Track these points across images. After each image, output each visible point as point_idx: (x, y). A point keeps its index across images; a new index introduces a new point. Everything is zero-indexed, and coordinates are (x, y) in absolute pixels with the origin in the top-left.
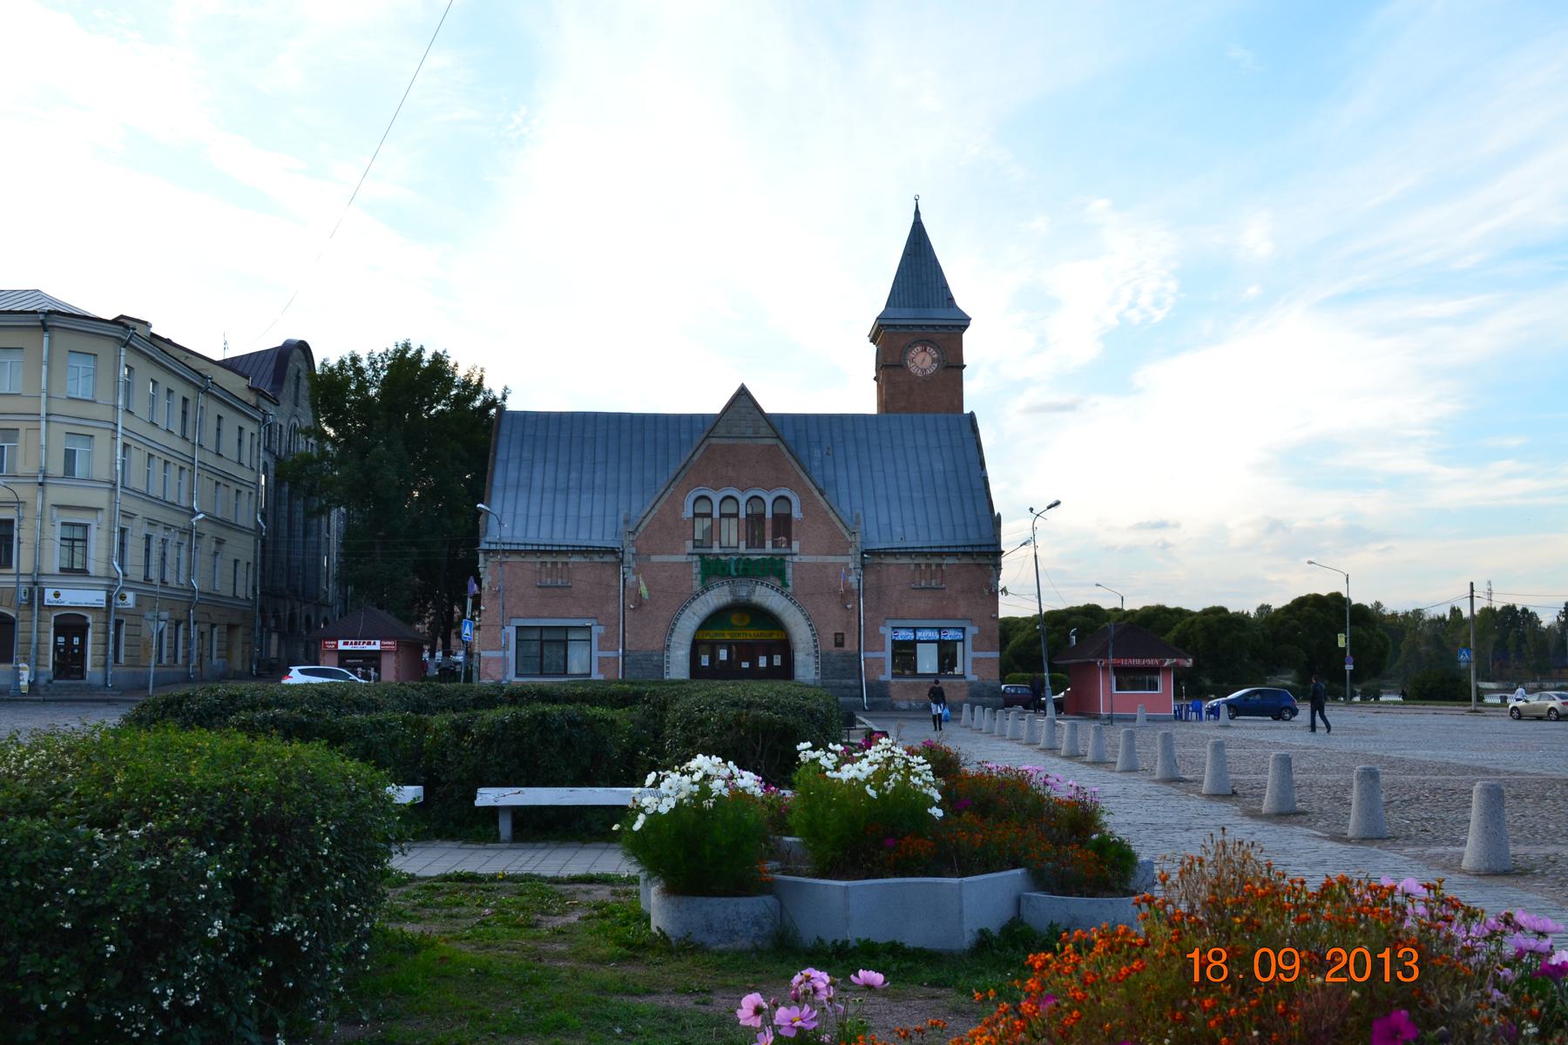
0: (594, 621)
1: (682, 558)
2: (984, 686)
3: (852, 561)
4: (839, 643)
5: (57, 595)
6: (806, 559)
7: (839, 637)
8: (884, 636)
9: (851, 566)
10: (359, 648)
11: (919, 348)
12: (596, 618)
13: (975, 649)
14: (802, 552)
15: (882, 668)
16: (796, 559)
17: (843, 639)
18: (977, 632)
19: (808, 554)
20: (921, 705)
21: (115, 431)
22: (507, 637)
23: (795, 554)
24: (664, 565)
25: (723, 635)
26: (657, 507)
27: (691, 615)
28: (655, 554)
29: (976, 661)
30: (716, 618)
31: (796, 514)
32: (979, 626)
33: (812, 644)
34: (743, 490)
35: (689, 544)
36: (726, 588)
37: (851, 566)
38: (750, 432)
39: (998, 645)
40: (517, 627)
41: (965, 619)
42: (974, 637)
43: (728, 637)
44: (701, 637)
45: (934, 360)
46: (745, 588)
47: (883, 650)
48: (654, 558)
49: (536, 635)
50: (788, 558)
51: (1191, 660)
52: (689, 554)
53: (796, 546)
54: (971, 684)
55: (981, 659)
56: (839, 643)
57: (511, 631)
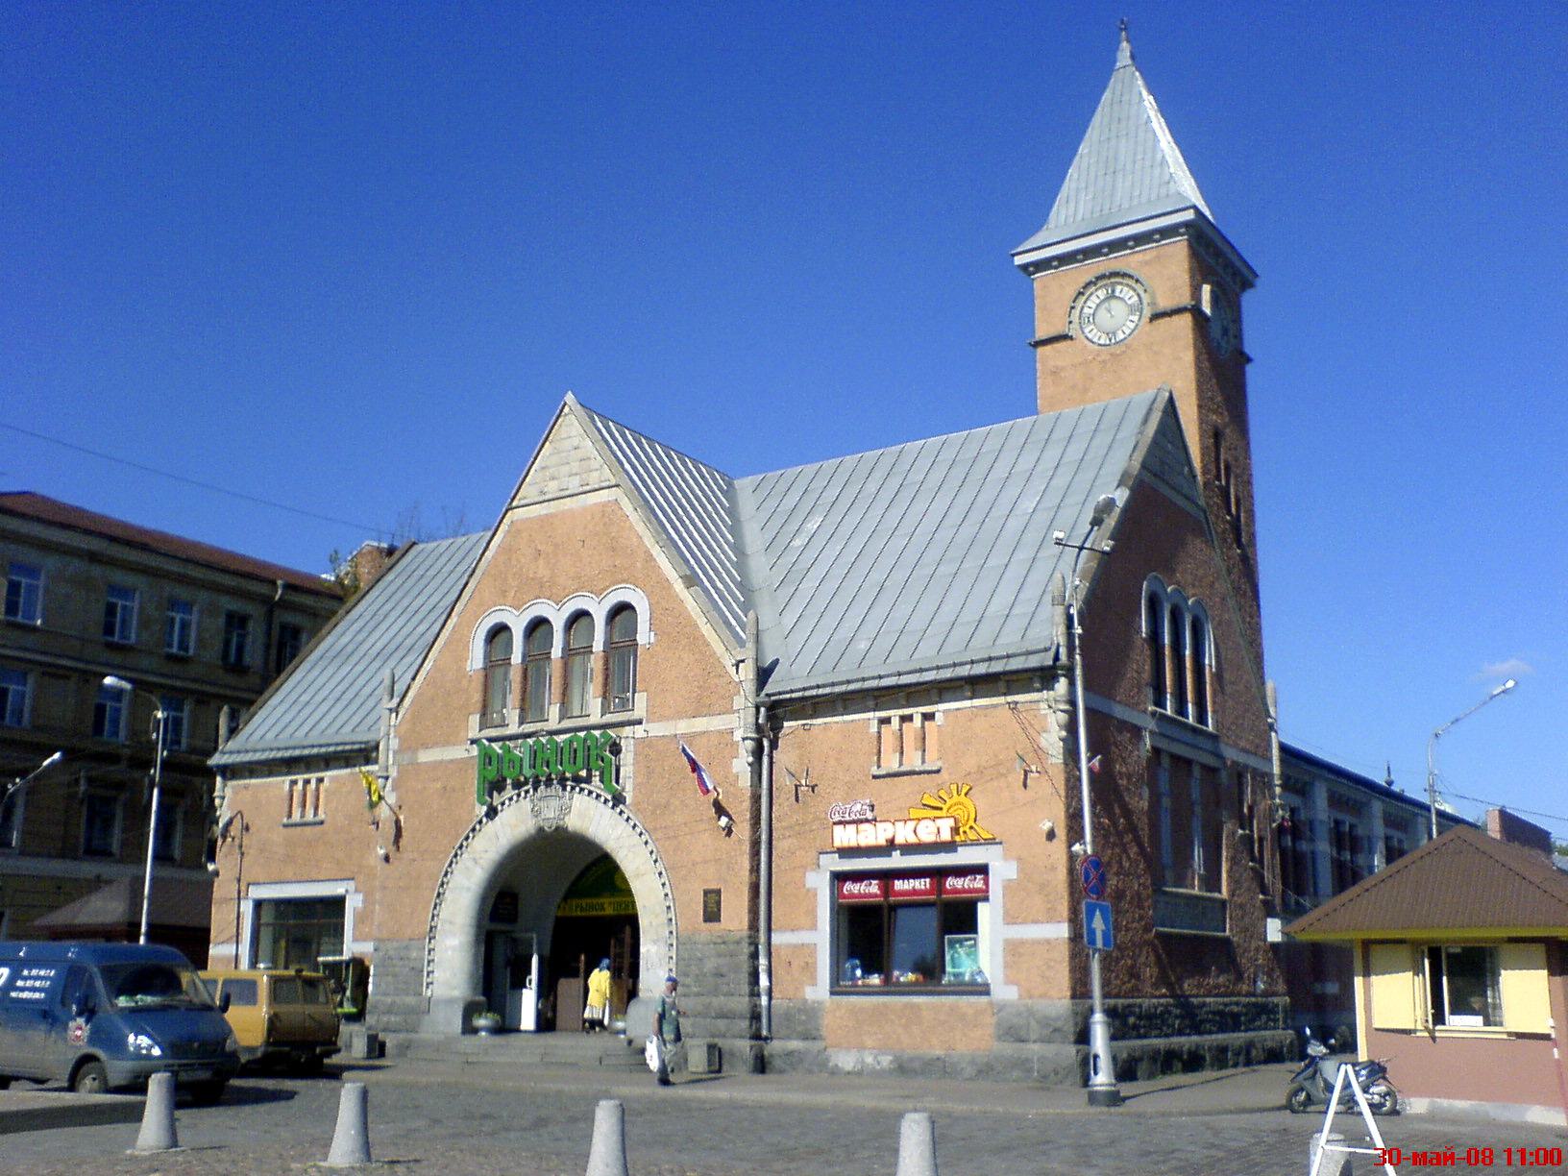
0: (351, 885)
2: (1031, 1013)
3: (739, 722)
4: (712, 914)
6: (657, 729)
7: (713, 897)
8: (813, 894)
9: (738, 735)
11: (1102, 294)
12: (353, 879)
13: (1010, 919)
14: (654, 715)
15: (810, 968)
16: (639, 731)
17: (719, 903)
19: (662, 718)
20: (886, 1061)
23: (640, 722)
25: (603, 909)
27: (470, 864)
28: (426, 746)
31: (644, 636)
32: (1019, 859)
33: (664, 918)
34: (559, 602)
35: (475, 720)
36: (526, 804)
37: (738, 735)
38: (574, 485)
39: (1063, 908)
43: (609, 911)
44: (568, 913)
45: (1132, 310)
46: (554, 803)
47: (814, 927)
48: (425, 757)
50: (627, 731)
52: (473, 742)
53: (640, 705)
54: (1002, 1007)
55: (1022, 943)
56: (712, 914)
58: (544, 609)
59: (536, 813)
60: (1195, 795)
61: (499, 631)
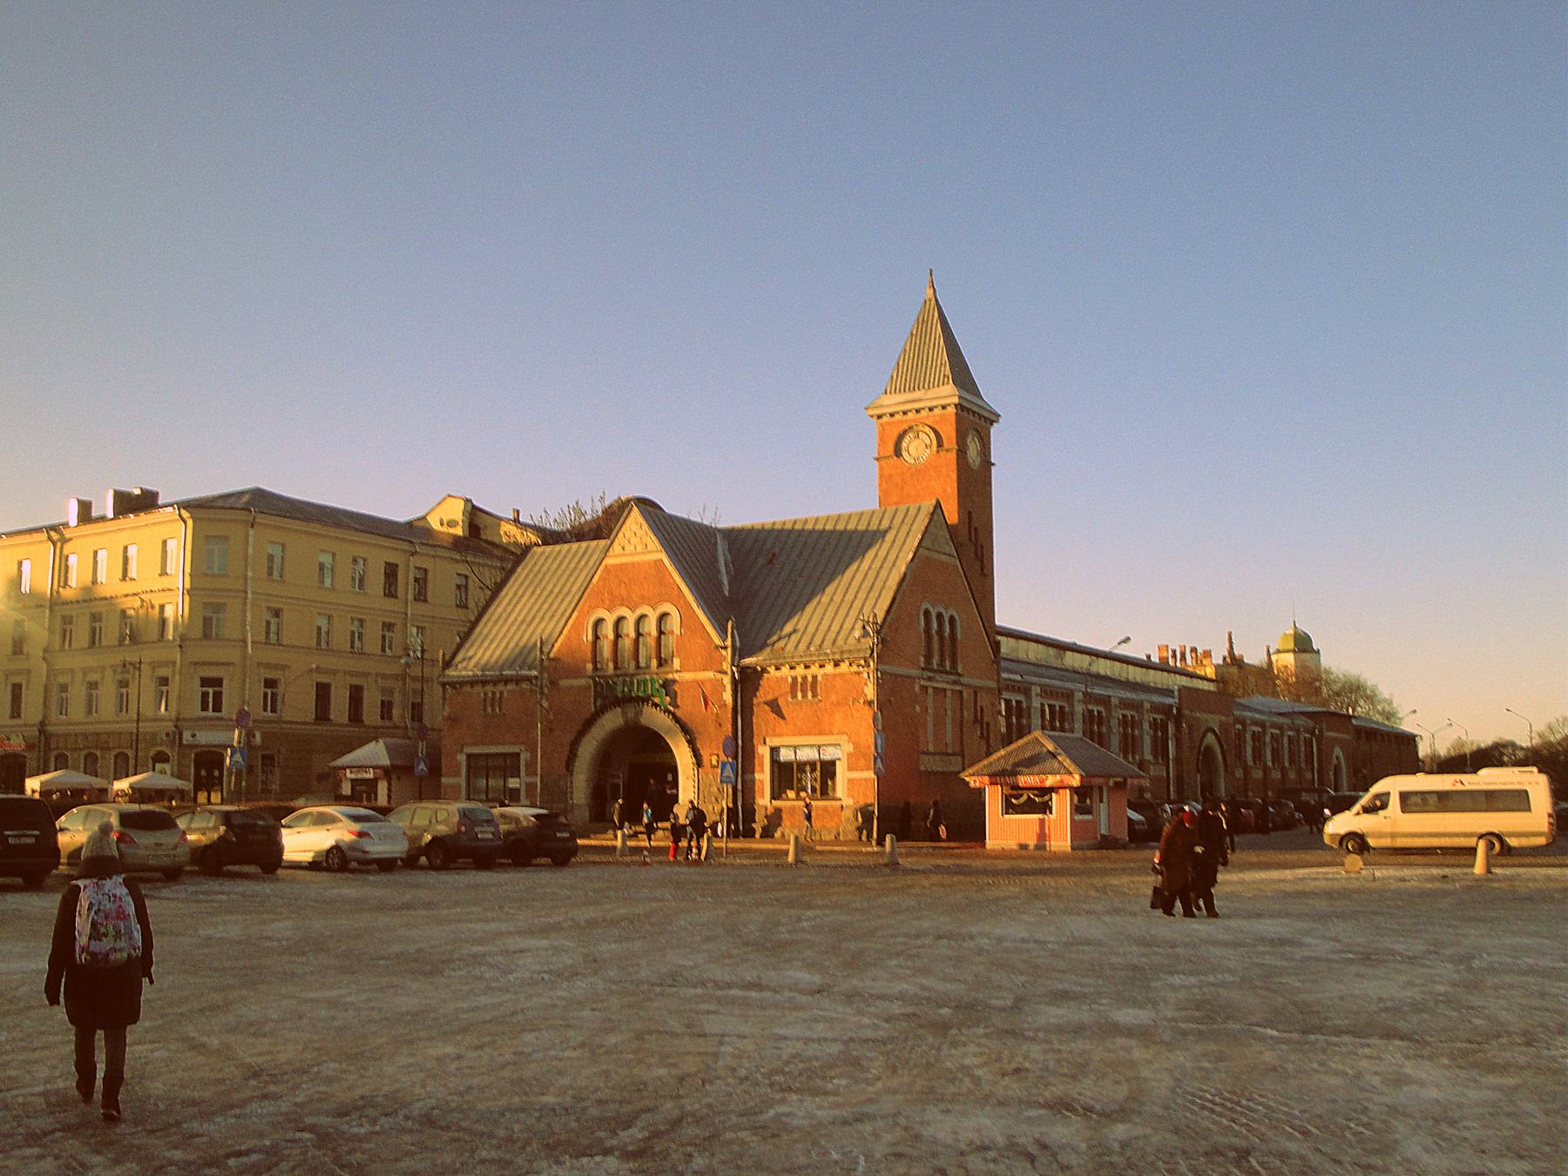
1: (582, 682)
5: (194, 736)
10: (359, 776)
13: (850, 768)
18: (852, 750)
21: (246, 598)
22: (458, 766)
24: (571, 688)
26: (565, 632)
29: (851, 781)
30: (615, 740)
40: (469, 756)
41: (841, 733)
42: (850, 755)
49: (482, 763)
51: (1077, 777)
57: (462, 758)
58: (624, 611)
59: (624, 714)
60: (949, 706)
61: (599, 622)
